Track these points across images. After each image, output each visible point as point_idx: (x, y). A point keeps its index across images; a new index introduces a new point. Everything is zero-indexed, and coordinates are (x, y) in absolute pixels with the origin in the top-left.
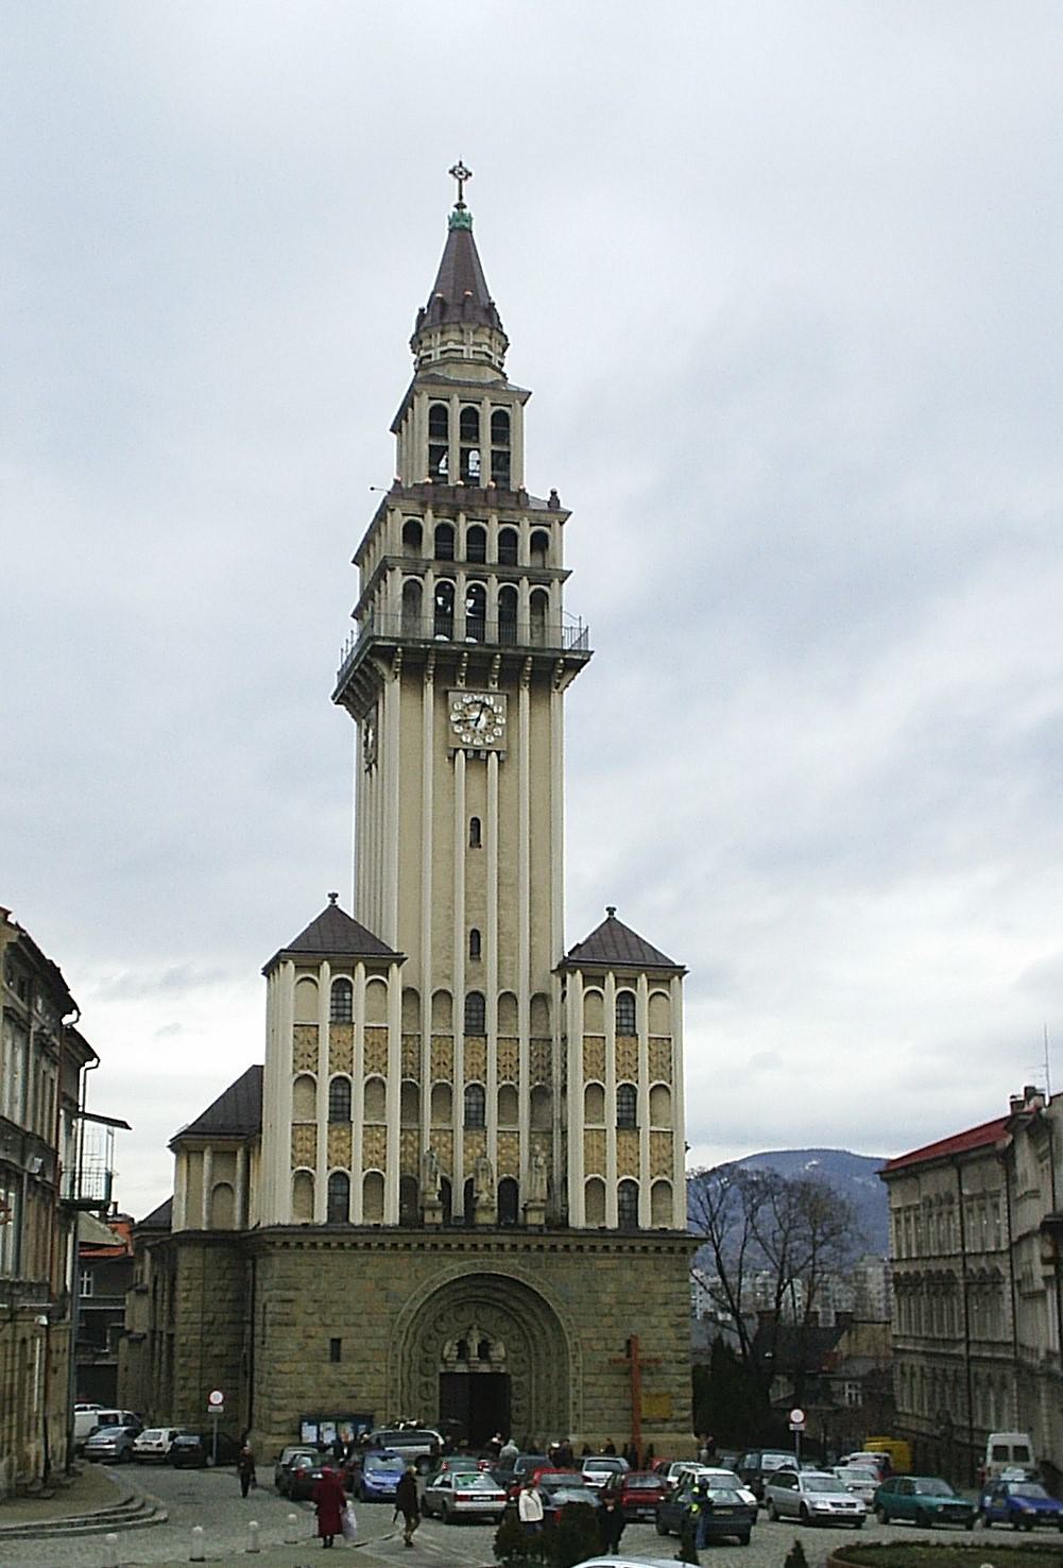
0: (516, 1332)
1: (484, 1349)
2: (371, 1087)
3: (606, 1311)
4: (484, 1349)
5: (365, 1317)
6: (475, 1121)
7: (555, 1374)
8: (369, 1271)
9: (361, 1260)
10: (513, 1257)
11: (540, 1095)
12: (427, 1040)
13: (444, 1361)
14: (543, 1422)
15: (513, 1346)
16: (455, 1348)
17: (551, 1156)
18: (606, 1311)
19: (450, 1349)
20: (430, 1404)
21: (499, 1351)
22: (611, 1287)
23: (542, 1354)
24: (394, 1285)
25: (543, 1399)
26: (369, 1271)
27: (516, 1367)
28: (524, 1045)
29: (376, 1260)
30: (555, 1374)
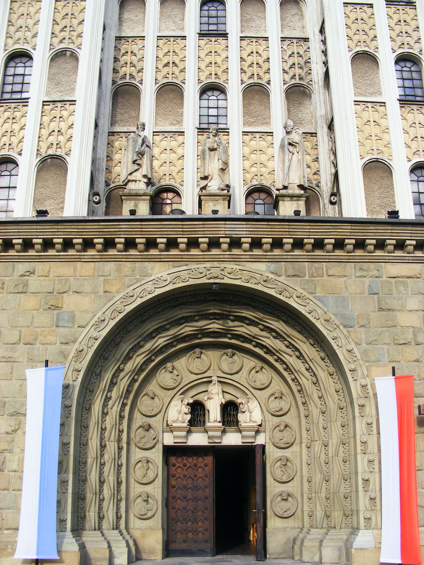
0: (277, 385)
1: (230, 410)
2: (61, 61)
3: (410, 337)
4: (230, 410)
5: (21, 347)
6: (212, 129)
7: (334, 442)
8: (34, 283)
9: (22, 267)
10: (256, 260)
11: (297, 93)
12: (150, 42)
13: (170, 429)
14: (319, 514)
15: (275, 405)
16: (186, 409)
17: (316, 160)
18: (410, 337)
19: (178, 412)
20: (149, 489)
21: (252, 414)
22: (413, 303)
23: (315, 412)
24: (70, 302)
25: (318, 478)
26: (34, 283)
27: (278, 435)
28: (275, 43)
29: (40, 267)
30: (334, 442)
